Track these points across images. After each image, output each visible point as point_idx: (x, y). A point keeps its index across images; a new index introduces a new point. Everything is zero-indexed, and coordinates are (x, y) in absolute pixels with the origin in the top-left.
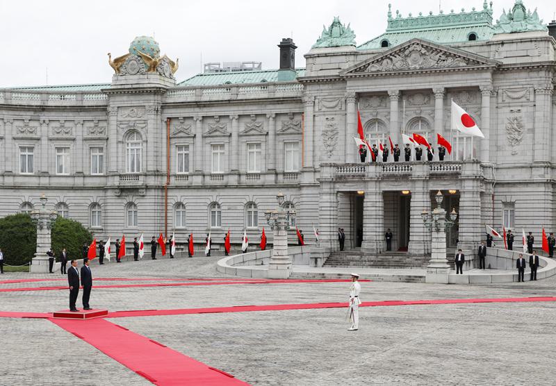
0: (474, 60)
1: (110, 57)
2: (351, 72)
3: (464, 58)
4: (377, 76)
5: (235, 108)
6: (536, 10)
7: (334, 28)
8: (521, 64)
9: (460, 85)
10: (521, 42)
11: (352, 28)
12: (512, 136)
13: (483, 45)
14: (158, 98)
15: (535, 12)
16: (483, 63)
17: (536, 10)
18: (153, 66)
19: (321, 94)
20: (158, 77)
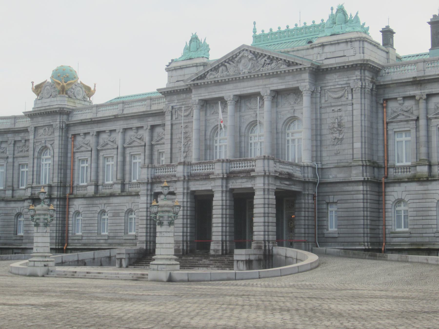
1: (33, 85)
2: (194, 80)
3: (285, 60)
4: (217, 83)
5: (121, 122)
6: (357, 13)
7: (192, 43)
8: (337, 63)
11: (208, 42)
12: (334, 135)
13: (308, 49)
14: (65, 117)
15: (356, 17)
16: (301, 64)
17: (357, 13)
18: (61, 90)
20: (66, 99)
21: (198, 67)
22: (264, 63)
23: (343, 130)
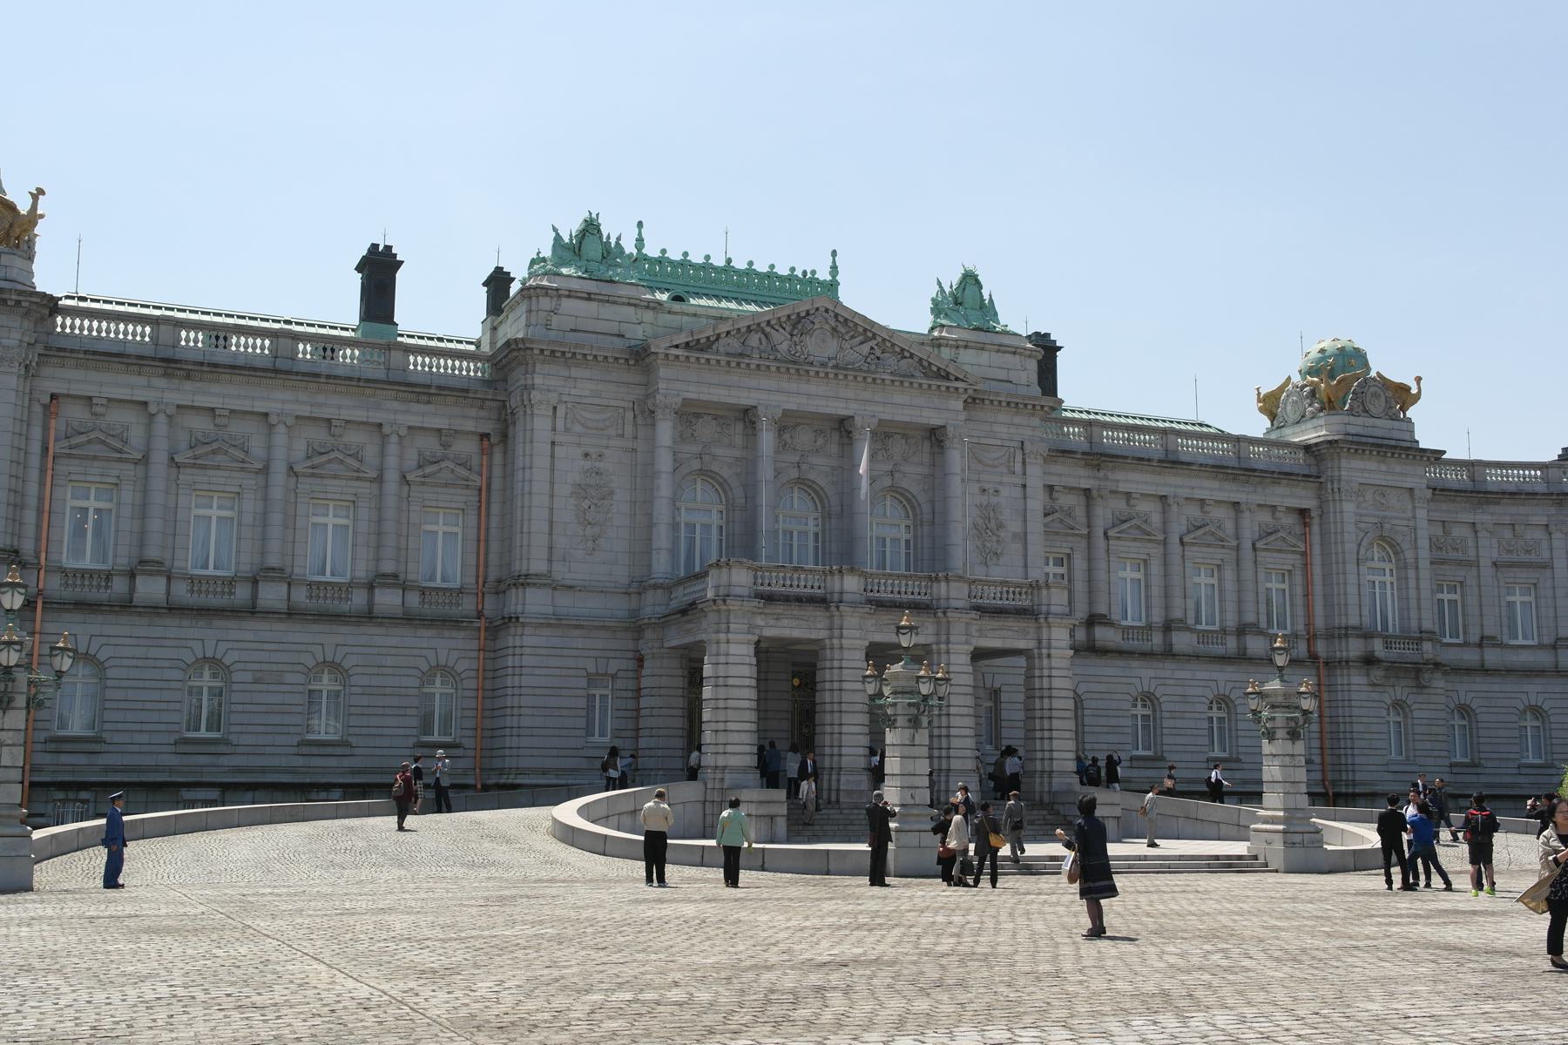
0: (939, 369)
2: (677, 346)
9: (907, 419)
10: (998, 351)
16: (957, 379)
19: (573, 391)
21: (639, 311)
22: (870, 353)
23: (1002, 535)
